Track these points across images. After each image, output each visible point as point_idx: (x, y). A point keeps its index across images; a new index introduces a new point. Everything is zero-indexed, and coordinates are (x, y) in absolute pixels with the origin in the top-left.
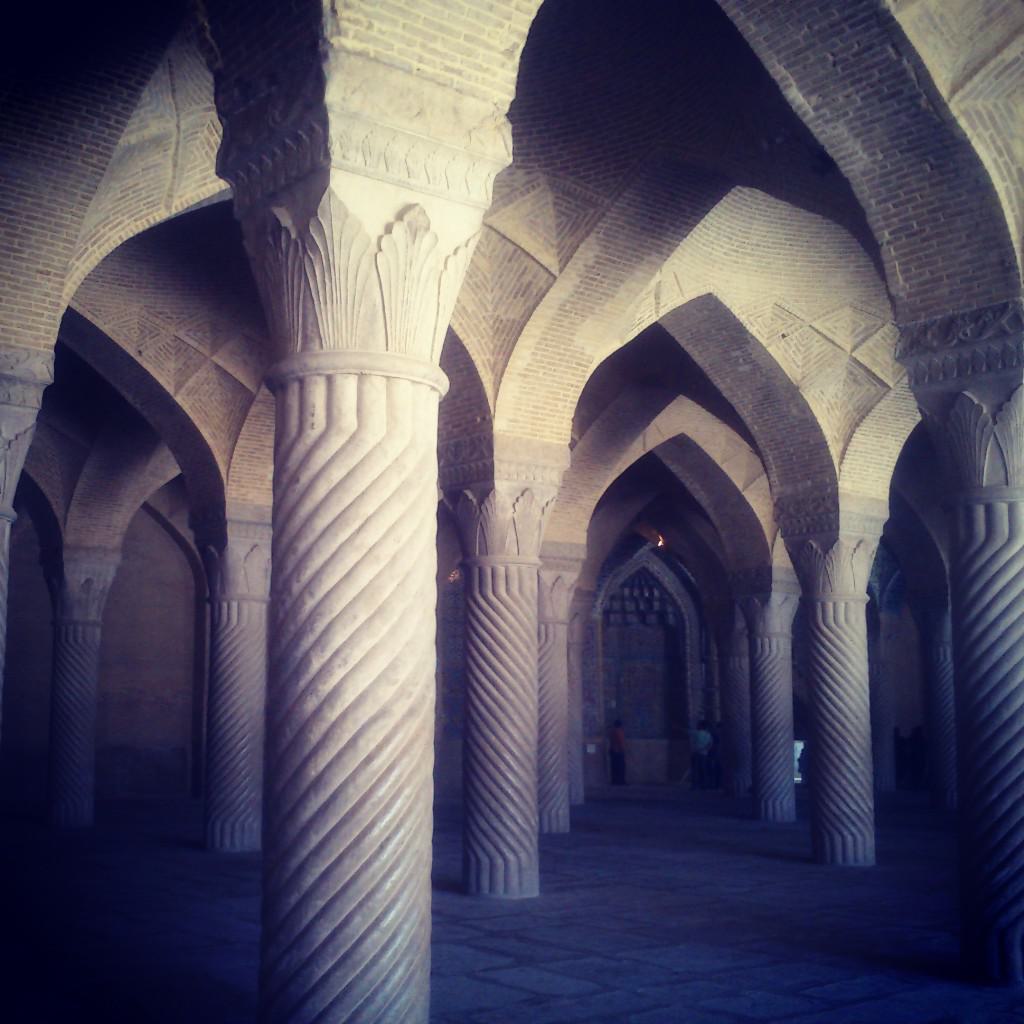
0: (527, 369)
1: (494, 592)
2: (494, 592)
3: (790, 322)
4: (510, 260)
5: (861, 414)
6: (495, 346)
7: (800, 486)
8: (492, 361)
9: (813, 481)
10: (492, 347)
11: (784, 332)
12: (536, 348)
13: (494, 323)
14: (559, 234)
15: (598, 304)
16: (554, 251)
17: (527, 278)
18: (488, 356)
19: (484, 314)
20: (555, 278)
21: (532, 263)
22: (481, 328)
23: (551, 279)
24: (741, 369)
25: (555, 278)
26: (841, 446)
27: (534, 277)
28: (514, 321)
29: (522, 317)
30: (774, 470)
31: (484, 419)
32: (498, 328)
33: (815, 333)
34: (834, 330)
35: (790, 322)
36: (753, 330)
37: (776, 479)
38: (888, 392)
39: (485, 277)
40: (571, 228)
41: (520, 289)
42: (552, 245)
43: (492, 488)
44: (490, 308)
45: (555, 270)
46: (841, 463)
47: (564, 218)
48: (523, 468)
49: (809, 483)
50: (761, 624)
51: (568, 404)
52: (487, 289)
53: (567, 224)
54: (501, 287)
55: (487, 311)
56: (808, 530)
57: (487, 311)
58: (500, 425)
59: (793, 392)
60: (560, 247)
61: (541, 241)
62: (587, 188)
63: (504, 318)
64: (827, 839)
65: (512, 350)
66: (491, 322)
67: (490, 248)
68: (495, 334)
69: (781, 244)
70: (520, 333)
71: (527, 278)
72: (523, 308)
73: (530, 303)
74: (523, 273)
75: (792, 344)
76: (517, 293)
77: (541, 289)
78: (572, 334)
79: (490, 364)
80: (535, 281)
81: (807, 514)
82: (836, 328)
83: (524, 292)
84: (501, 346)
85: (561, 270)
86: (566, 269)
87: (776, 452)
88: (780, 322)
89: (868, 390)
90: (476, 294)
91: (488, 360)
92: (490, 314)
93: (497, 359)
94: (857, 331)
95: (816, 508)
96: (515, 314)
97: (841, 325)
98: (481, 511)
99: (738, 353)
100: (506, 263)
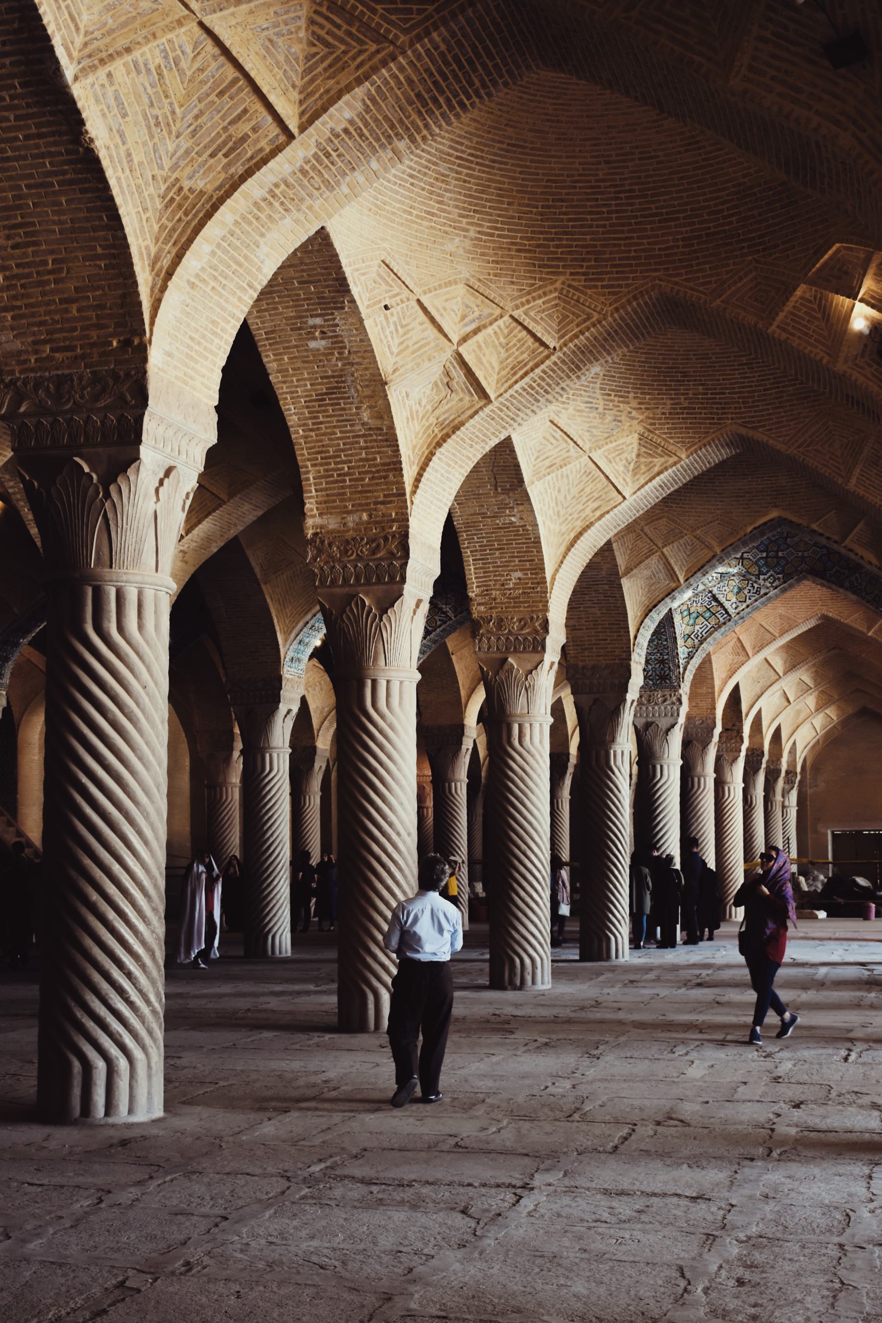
0: (197, 276)
1: (121, 629)
2: (121, 629)
3: (396, 290)
4: (221, 94)
5: (444, 432)
6: (163, 228)
7: (351, 520)
8: (153, 250)
9: (370, 516)
10: (156, 227)
11: (387, 302)
12: (219, 246)
13: (169, 189)
14: (308, 71)
15: (310, 196)
16: (295, 95)
17: (244, 128)
18: (148, 242)
19: (156, 172)
20: (291, 137)
21: (258, 106)
22: (146, 194)
23: (282, 138)
24: (313, 344)
25: (291, 137)
26: (415, 469)
27: (254, 129)
28: (202, 193)
29: (219, 188)
30: (314, 493)
31: (126, 343)
32: (172, 200)
33: (420, 312)
34: (442, 311)
35: (396, 290)
36: (355, 290)
37: (314, 507)
38: (485, 406)
39: (173, 112)
40: (330, 66)
41: (225, 143)
42: (294, 86)
43: (135, 458)
44: (167, 163)
45: (293, 125)
46: (414, 492)
47: (322, 50)
48: (170, 433)
49: (365, 516)
50: (522, 700)
51: (222, 344)
52: (170, 133)
53: (322, 60)
54: (194, 134)
55: (161, 168)
56: (358, 579)
57: (161, 168)
58: (157, 359)
59: (377, 385)
60: (306, 94)
61: (280, 73)
62: (374, 11)
63: (186, 184)
64: (371, 998)
65: (190, 241)
66: (163, 188)
67: (197, 65)
68: (166, 207)
69: (402, 179)
70: (209, 215)
71: (244, 128)
72: (223, 176)
73: (239, 169)
74: (239, 117)
75: (391, 320)
76: (219, 149)
77: (261, 150)
78: (262, 235)
79: (149, 255)
80: (253, 136)
81: (359, 558)
82: (445, 309)
83: (232, 149)
84: (174, 229)
85: (303, 129)
86: (311, 130)
87: (322, 468)
88: (384, 287)
89: (461, 400)
90: (152, 137)
91: (147, 248)
92: (164, 173)
93: (160, 250)
94: (467, 320)
95: (374, 552)
96: (204, 182)
97: (453, 307)
98: (107, 495)
99: (318, 321)
100: (213, 97)
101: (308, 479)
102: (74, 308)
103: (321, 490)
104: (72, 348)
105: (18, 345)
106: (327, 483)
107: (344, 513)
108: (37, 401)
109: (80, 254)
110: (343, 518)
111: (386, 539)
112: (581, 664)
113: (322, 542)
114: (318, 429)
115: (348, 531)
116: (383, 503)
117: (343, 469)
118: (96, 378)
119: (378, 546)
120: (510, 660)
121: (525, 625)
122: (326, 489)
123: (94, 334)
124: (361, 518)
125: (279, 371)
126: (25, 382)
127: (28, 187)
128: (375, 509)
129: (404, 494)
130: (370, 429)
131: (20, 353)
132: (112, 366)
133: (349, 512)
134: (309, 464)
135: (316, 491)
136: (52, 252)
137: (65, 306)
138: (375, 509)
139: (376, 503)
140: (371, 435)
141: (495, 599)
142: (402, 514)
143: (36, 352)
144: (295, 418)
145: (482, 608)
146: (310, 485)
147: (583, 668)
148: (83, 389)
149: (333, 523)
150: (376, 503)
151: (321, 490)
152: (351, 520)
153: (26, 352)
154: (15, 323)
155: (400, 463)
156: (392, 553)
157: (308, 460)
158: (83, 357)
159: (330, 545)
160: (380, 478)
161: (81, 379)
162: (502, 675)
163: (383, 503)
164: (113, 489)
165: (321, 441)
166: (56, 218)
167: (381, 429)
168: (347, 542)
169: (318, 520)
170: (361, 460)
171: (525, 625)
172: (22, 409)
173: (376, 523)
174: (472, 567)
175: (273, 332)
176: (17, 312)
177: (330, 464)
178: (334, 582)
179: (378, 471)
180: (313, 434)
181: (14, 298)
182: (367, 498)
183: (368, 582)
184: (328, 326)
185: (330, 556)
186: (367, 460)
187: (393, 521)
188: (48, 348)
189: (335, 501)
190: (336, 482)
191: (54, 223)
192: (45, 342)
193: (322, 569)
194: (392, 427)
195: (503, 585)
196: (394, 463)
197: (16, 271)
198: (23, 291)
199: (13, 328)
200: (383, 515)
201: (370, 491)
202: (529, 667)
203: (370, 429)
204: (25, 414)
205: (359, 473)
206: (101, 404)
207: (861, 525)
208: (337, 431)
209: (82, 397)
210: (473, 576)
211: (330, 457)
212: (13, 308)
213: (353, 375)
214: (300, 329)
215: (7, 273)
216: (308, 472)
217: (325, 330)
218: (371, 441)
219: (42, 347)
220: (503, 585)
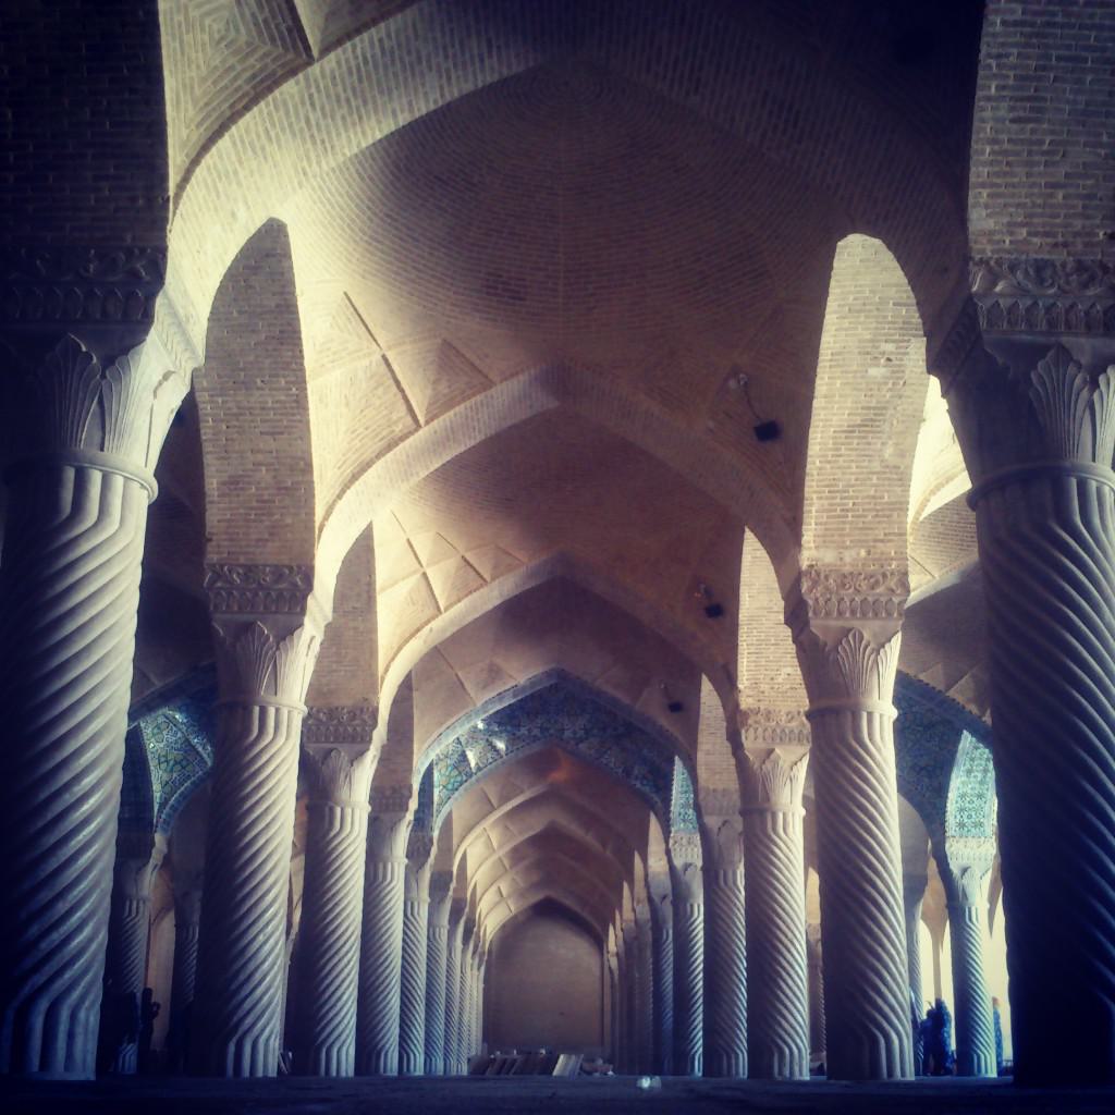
30: (813, 526)
37: (812, 539)
49: (863, 553)
87: (826, 502)
99: (890, 347)
101: (810, 511)
102: (1060, 194)
103: (821, 524)
104: (1054, 235)
105: (990, 224)
106: (828, 517)
107: (843, 548)
108: (1015, 282)
109: (1082, 140)
110: (840, 553)
111: (884, 576)
112: (711, 787)
113: (818, 574)
114: (836, 462)
115: (845, 565)
116: (882, 541)
117: (848, 504)
118: (1081, 267)
119: (877, 582)
120: (778, 751)
121: (792, 718)
122: (826, 523)
123: (1078, 224)
124: (858, 554)
125: (825, 397)
126: (999, 262)
127: (1059, 58)
128: (874, 547)
129: (905, 534)
130: (887, 467)
131: (992, 233)
132: (1099, 257)
133: (847, 548)
134: (815, 496)
135: (816, 524)
136: (1052, 132)
137: (1049, 191)
138: (874, 547)
139: (875, 541)
140: (885, 473)
141: (763, 692)
142: (902, 553)
143: (1011, 234)
144: (818, 447)
145: (750, 700)
146: (811, 518)
147: (714, 791)
148: (1068, 275)
149: (828, 557)
150: (875, 541)
151: (821, 524)
152: (848, 556)
153: (1001, 232)
154: (990, 201)
155: (908, 503)
156: (893, 591)
157: (815, 492)
158: (1065, 245)
159: (827, 577)
160: (884, 516)
161: (1064, 265)
162: (768, 766)
163: (882, 541)
164: (1102, 379)
165: (834, 474)
166: (1071, 97)
167: (899, 468)
168: (845, 576)
169: (814, 553)
170: (868, 497)
171: (792, 718)
172: (998, 289)
173: (874, 560)
174: (745, 660)
175: (839, 354)
176: (994, 190)
177: (836, 498)
178: (828, 614)
179: (882, 510)
180: (828, 466)
181: (997, 174)
182: (867, 535)
183: (864, 615)
184: (898, 354)
185: (827, 588)
186: (874, 497)
187: (892, 559)
188: (1024, 231)
189: (833, 536)
190: (839, 517)
191: (1068, 102)
192: (1022, 225)
193: (817, 599)
194: (909, 467)
195: (772, 679)
196: (901, 503)
197: (1006, 146)
198: (1008, 169)
199: (986, 206)
200: (882, 553)
201: (872, 529)
202: (794, 759)
203: (887, 467)
204: (1001, 295)
205: (864, 510)
206: (1091, 292)
207: (966, 677)
208: (854, 465)
209: (1068, 283)
210: (745, 668)
211: (838, 492)
212: (993, 185)
213: (895, 408)
214: (868, 353)
215: (996, 147)
216: (811, 505)
217: (892, 357)
218: (884, 479)
219: (1017, 230)
220: (772, 679)
